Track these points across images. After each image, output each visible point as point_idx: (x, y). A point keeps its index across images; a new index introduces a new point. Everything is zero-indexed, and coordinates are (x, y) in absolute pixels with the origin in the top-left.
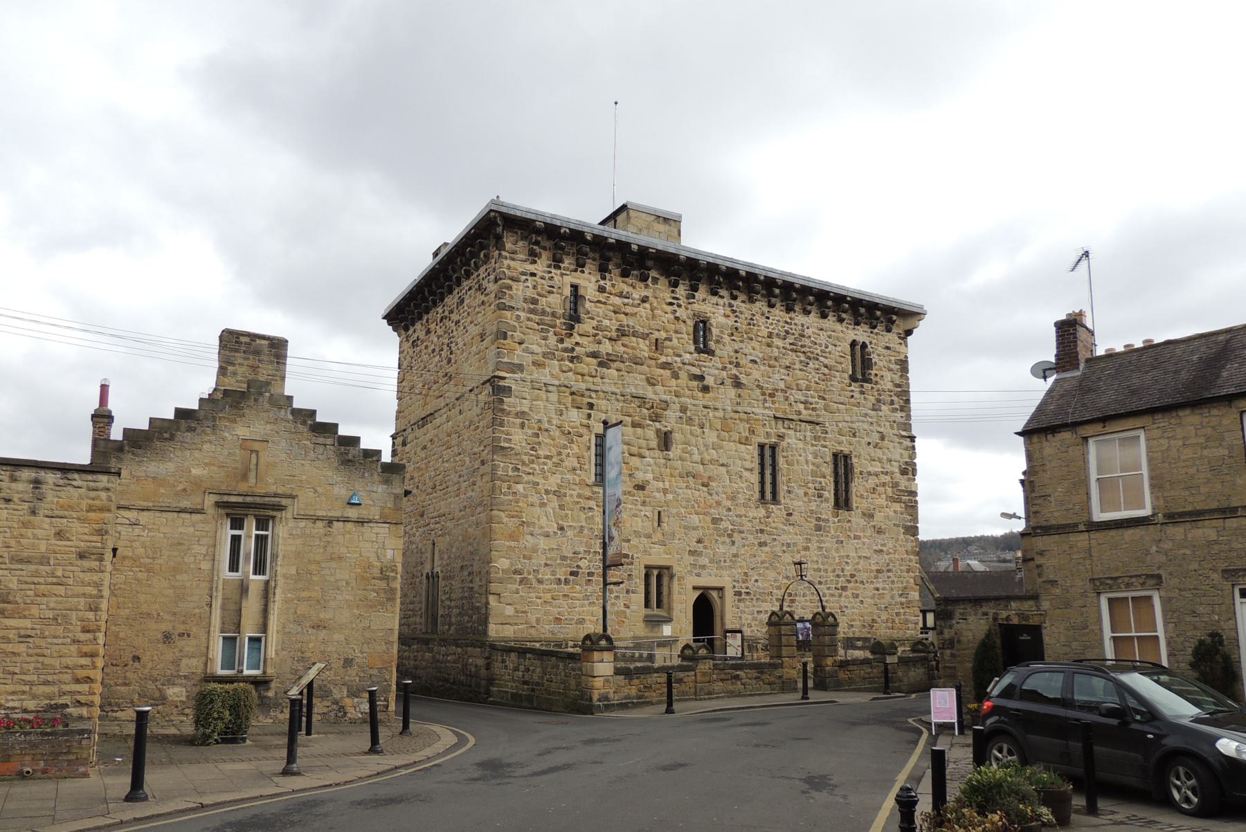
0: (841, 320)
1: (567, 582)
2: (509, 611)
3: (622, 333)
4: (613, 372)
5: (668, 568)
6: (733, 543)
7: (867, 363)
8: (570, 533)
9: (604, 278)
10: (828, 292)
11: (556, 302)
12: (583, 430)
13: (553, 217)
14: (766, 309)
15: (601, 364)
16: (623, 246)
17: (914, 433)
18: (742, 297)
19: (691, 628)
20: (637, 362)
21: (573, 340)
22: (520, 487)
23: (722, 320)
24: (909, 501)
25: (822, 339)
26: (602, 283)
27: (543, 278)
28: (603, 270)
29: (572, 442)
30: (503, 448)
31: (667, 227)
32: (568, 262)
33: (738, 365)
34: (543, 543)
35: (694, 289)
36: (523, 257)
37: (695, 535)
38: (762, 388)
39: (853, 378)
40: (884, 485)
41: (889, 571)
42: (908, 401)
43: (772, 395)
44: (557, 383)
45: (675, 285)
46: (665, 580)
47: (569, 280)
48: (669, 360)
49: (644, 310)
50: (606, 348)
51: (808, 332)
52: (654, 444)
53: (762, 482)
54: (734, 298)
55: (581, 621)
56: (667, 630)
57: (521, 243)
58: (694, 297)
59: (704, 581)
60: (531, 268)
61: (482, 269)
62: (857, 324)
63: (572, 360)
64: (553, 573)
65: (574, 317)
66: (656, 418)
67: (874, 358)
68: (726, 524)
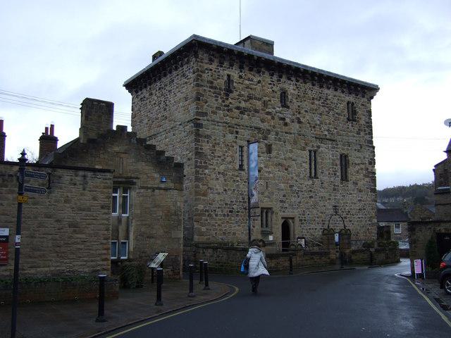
0: (343, 92)
1: (228, 215)
2: (204, 229)
3: (250, 98)
4: (245, 116)
5: (270, 209)
6: (299, 197)
7: (354, 113)
8: (229, 192)
9: (241, 72)
10: (338, 79)
11: (221, 83)
12: (234, 144)
13: (221, 43)
14: (311, 86)
15: (241, 113)
16: (250, 57)
17: (374, 145)
18: (301, 81)
19: (281, 237)
20: (257, 111)
21: (228, 102)
22: (207, 171)
23: (292, 91)
24: (372, 176)
25: (335, 101)
26: (241, 74)
27: (215, 71)
28: (241, 68)
29: (229, 149)
30: (200, 153)
31: (268, 47)
32: (226, 64)
33: (299, 113)
34: (217, 197)
35: (281, 77)
36: (206, 61)
37: (282, 193)
38: (310, 124)
39: (348, 119)
40: (362, 169)
41: (365, 209)
42: (371, 130)
43: (314, 127)
44: (222, 121)
45: (272, 75)
46: (269, 215)
47: (226, 72)
48: (270, 110)
49: (259, 87)
50: (243, 105)
51: (329, 97)
52: (265, 149)
53: (310, 169)
54: (298, 81)
55: (234, 234)
56: (271, 238)
57: (205, 55)
58: (280, 81)
59: (288, 214)
60: (210, 67)
61: (185, 67)
62: (350, 94)
63: (228, 110)
64: (222, 211)
65: (229, 91)
66: (265, 138)
67: (357, 109)
68: (295, 188)
